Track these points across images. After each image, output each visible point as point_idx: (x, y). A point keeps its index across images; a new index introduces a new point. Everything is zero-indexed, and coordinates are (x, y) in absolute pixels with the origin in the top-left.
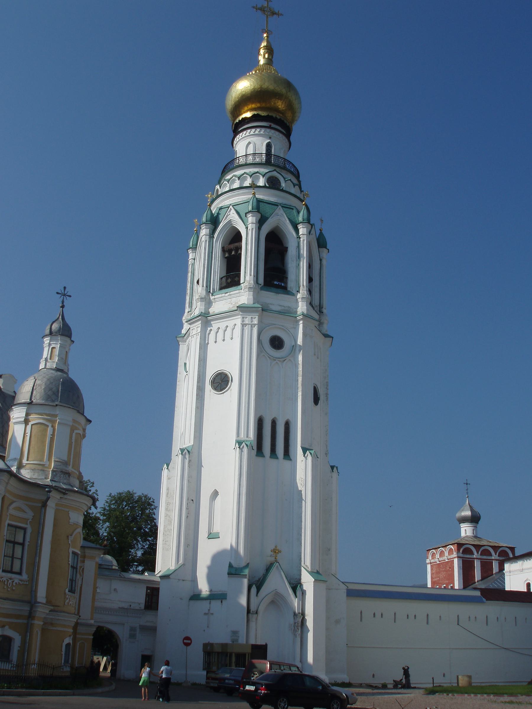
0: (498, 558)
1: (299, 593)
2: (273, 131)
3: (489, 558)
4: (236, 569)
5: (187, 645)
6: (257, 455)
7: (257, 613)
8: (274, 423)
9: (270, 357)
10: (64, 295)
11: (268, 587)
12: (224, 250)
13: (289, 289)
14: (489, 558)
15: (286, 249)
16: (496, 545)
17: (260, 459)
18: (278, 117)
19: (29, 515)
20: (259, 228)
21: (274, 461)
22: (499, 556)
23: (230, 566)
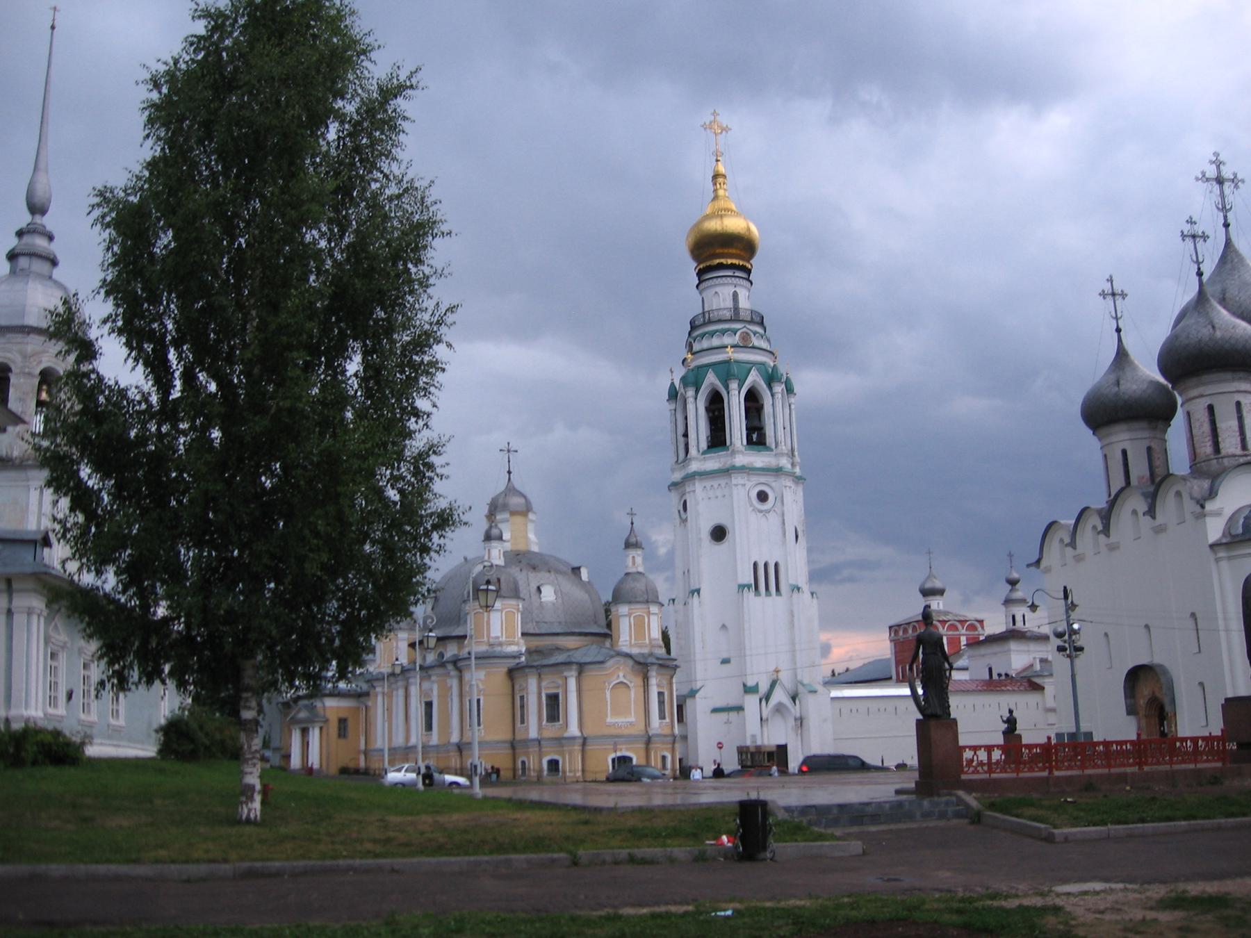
0: (964, 631)
1: (797, 702)
2: (737, 279)
3: (958, 633)
4: (750, 688)
5: (720, 748)
6: (755, 595)
7: (767, 720)
8: (766, 565)
9: (761, 511)
10: (632, 514)
11: (774, 700)
12: (707, 409)
13: (768, 444)
14: (958, 633)
15: (762, 407)
16: (962, 619)
17: (758, 599)
18: (741, 263)
19: (665, 682)
20: (739, 392)
21: (769, 599)
22: (966, 630)
23: (745, 685)
